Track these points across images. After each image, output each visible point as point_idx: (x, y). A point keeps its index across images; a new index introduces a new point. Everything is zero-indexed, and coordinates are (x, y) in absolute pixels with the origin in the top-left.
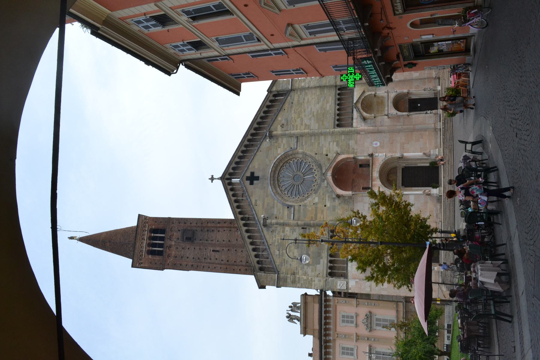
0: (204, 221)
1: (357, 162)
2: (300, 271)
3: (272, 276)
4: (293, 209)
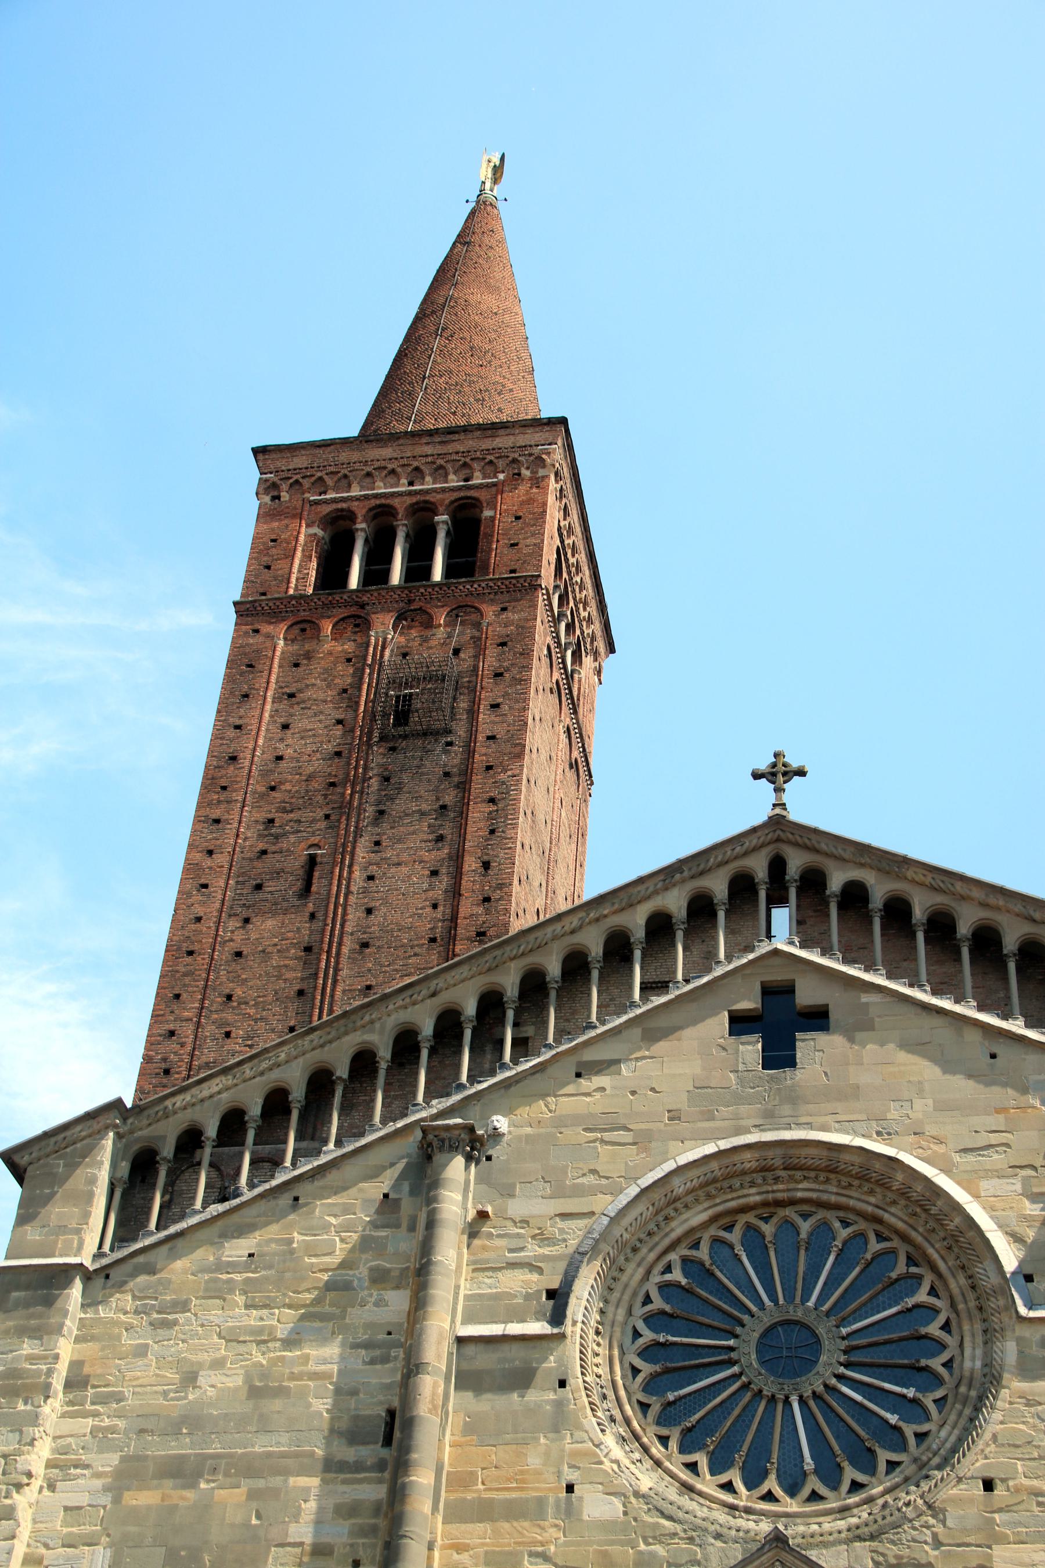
2: (90, 1421)
4: (537, 1327)
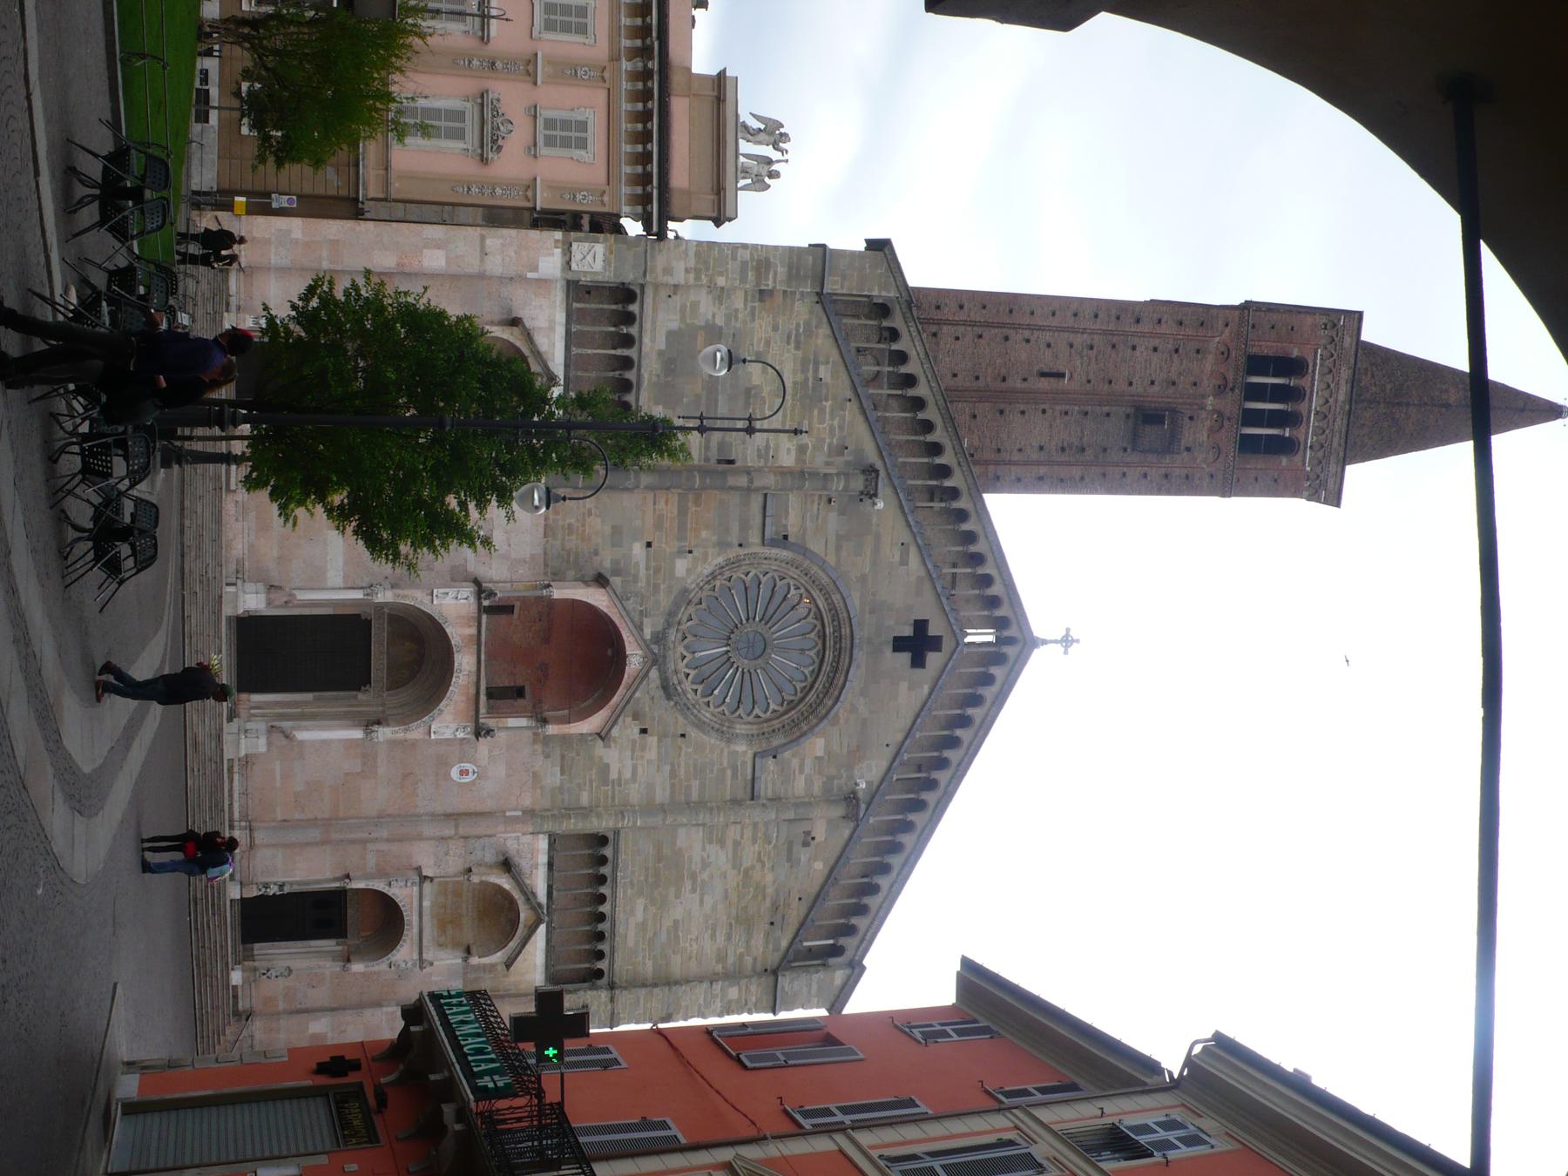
1: (534, 706)
3: (842, 287)
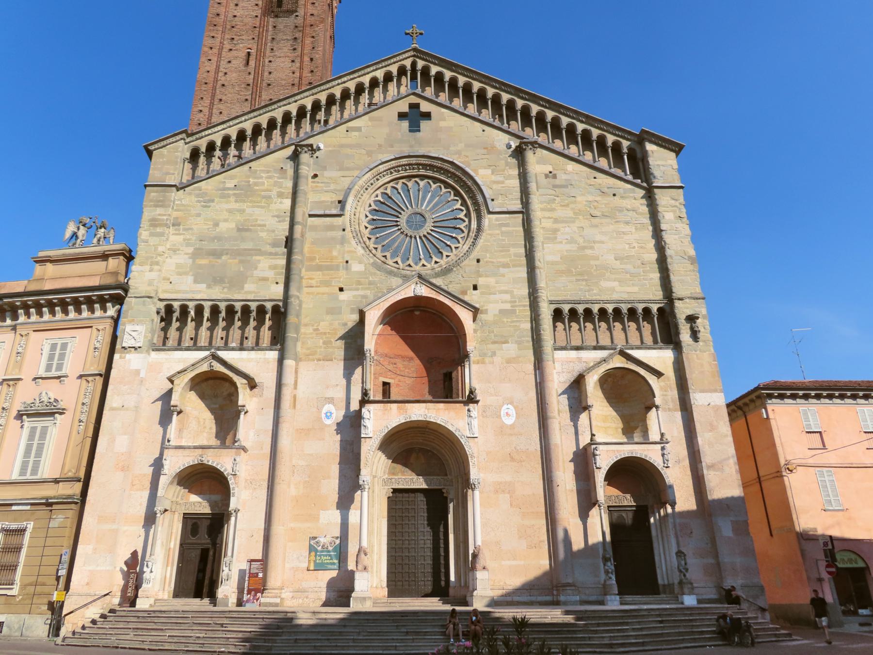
0: (316, 29)
4: (334, 212)
